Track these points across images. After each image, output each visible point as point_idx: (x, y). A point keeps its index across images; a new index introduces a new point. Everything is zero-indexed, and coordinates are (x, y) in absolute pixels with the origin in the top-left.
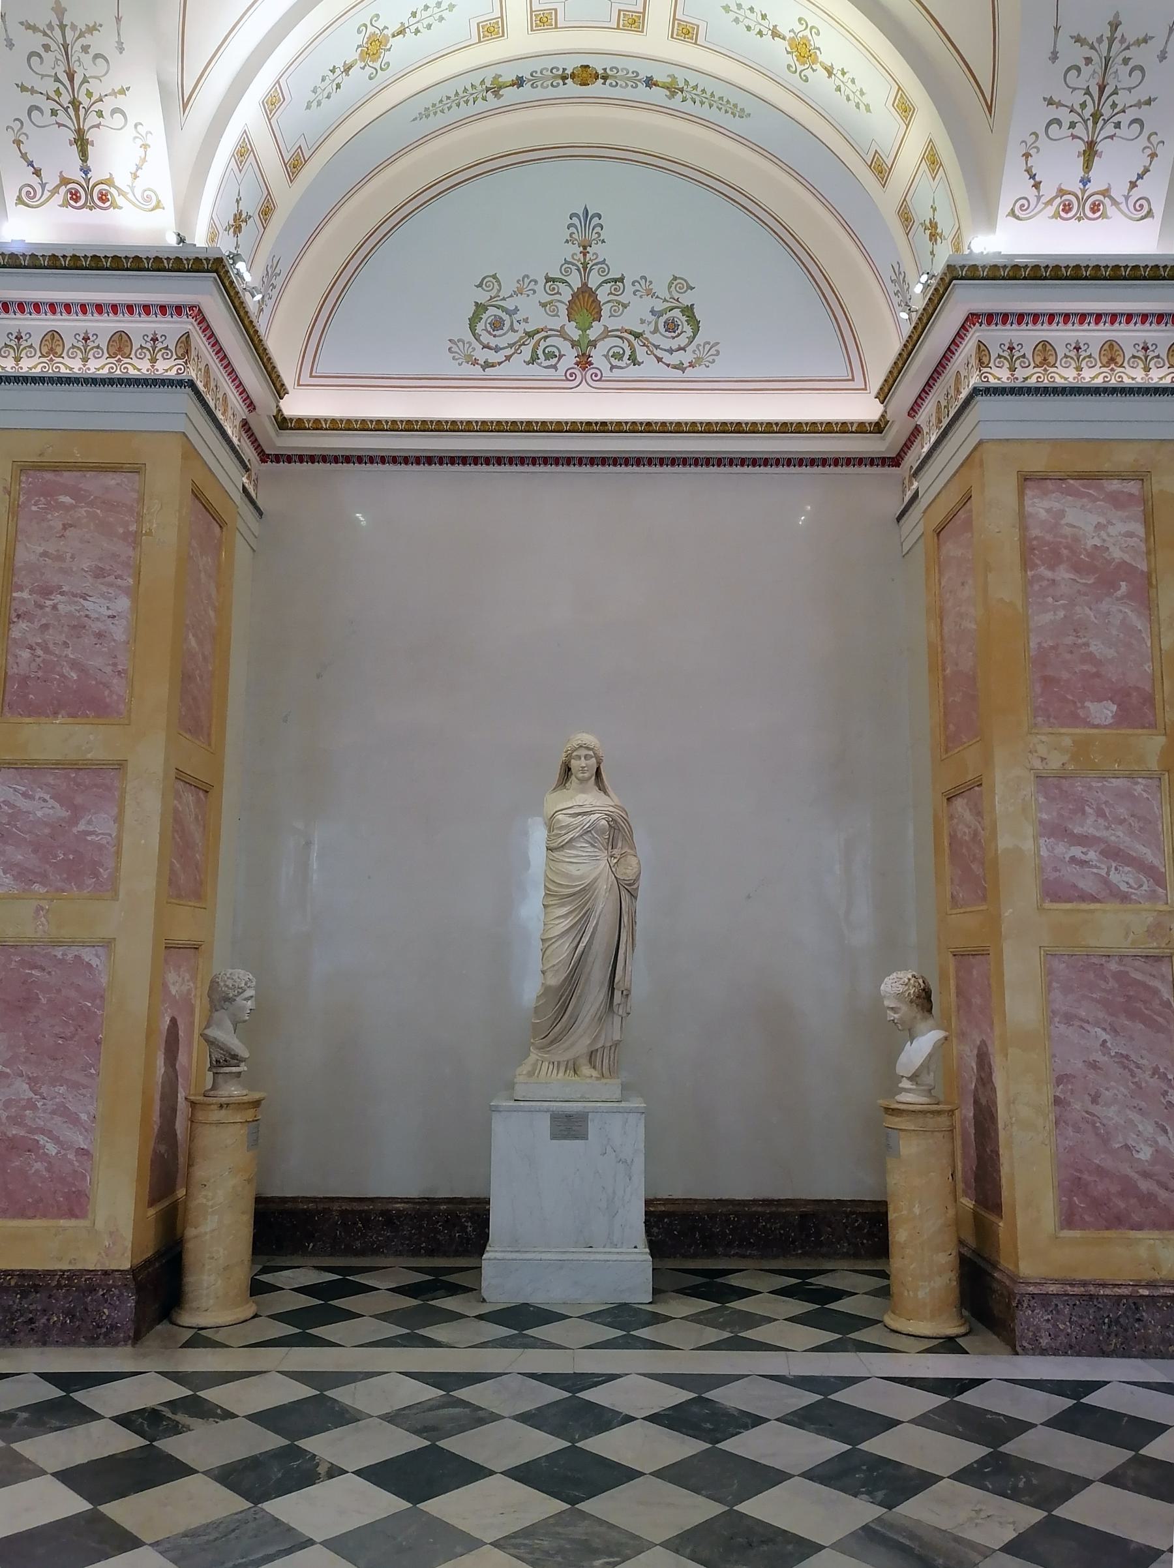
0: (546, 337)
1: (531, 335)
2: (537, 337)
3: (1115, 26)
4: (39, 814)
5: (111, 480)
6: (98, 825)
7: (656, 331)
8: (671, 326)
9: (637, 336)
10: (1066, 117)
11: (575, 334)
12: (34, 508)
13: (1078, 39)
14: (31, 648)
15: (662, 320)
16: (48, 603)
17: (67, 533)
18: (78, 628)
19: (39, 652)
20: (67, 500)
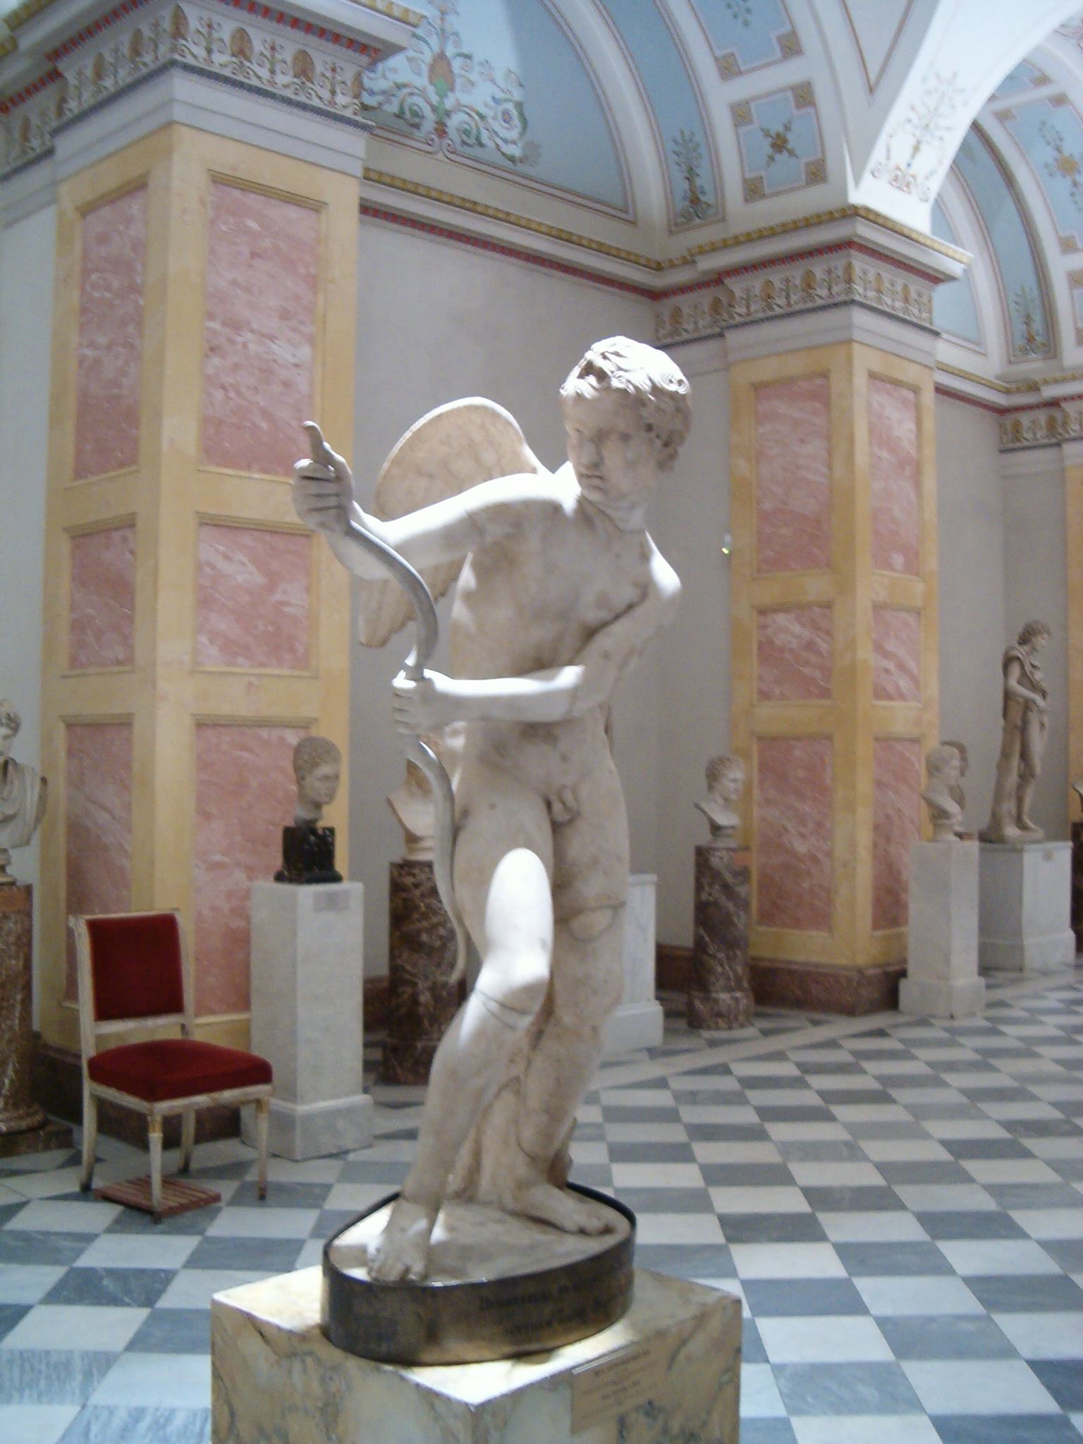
0: (411, 94)
1: (399, 86)
2: (405, 91)
3: (955, 75)
4: (240, 578)
5: (293, 212)
6: (292, 595)
7: (495, 118)
8: (507, 117)
9: (482, 117)
10: (915, 121)
11: (435, 99)
12: (224, 228)
13: (938, 76)
14: (224, 388)
15: (500, 108)
16: (240, 339)
17: (257, 263)
18: (267, 371)
19: (232, 394)
20: (252, 224)
